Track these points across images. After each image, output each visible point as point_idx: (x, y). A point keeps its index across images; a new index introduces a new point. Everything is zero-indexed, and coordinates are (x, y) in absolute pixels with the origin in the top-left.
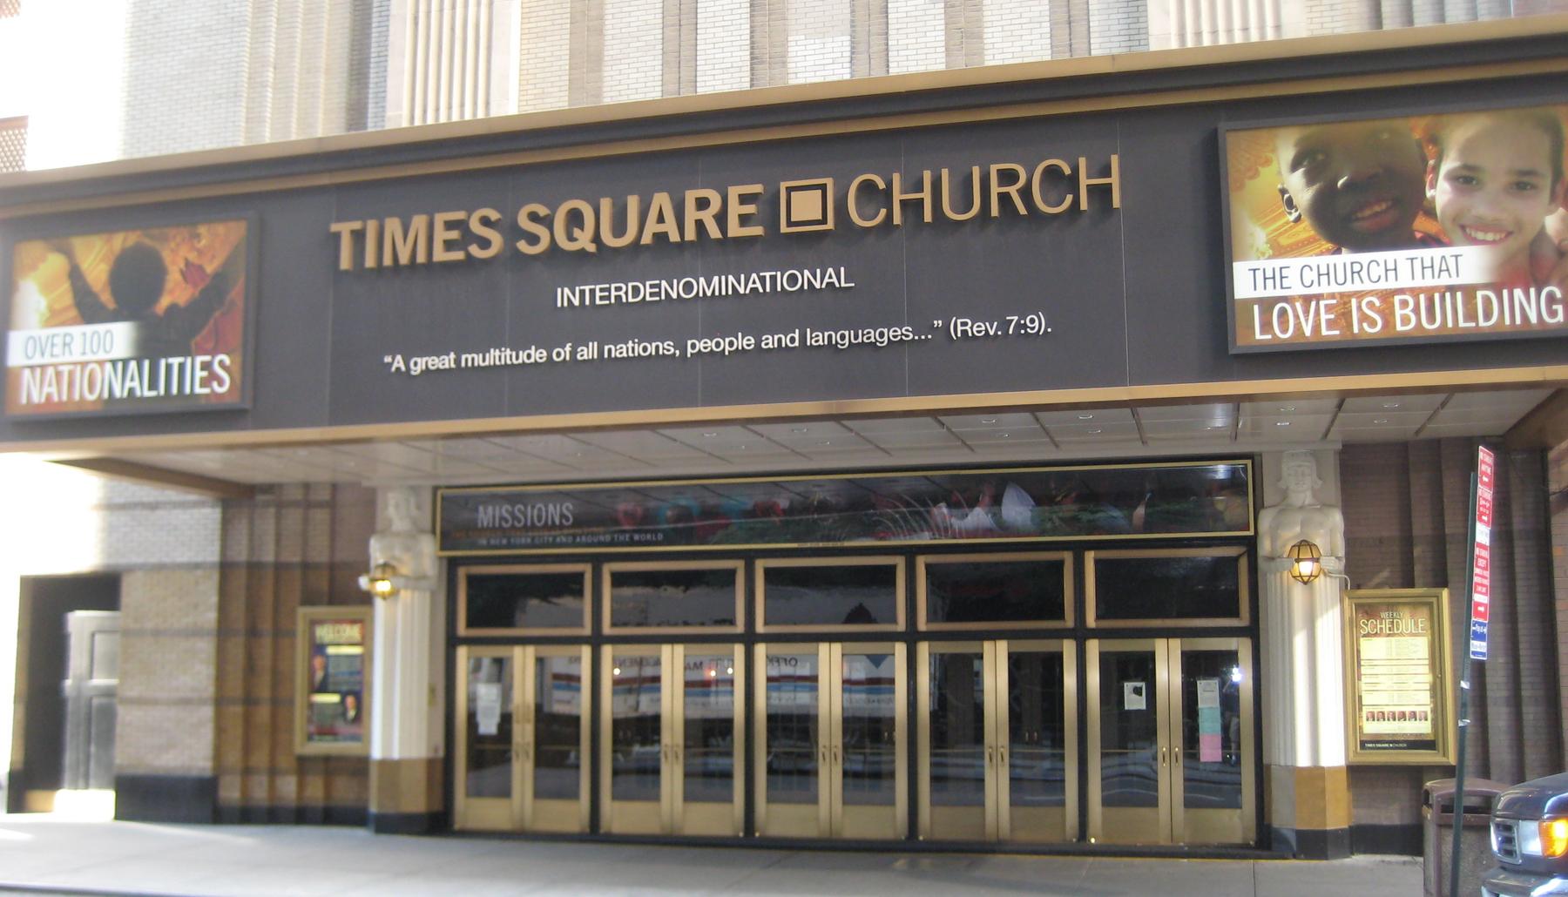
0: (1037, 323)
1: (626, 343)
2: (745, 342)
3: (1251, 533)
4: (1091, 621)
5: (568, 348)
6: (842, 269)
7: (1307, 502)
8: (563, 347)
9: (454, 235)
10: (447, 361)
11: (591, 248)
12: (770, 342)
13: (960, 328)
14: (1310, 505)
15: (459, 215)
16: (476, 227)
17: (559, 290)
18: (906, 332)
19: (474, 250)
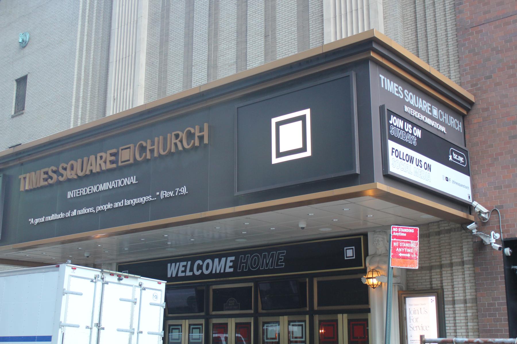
0: (184, 190)
1: (82, 209)
2: (109, 206)
3: (363, 267)
4: (316, 307)
5: (69, 212)
6: (135, 177)
7: (383, 252)
8: (68, 212)
9: (46, 176)
10: (42, 220)
11: (75, 177)
12: (116, 205)
13: (163, 194)
14: (384, 254)
15: (46, 170)
16: (50, 173)
17: (68, 192)
18: (149, 198)
19: (49, 180)
